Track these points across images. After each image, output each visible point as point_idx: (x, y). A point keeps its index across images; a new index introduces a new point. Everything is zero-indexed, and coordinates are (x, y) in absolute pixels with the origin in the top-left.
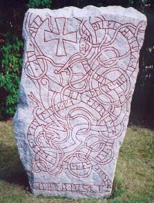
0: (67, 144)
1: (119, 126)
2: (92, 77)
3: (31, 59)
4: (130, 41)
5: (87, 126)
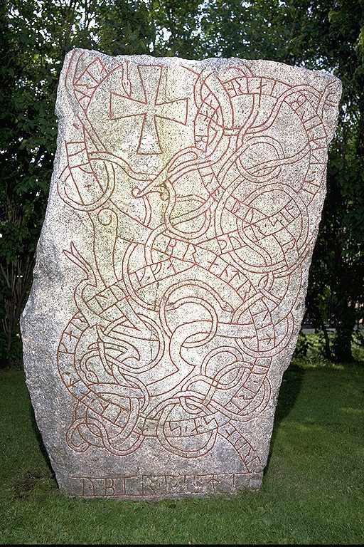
0: (159, 373)
1: (284, 323)
2: (221, 205)
3: (76, 161)
4: (308, 125)
5: (207, 326)
